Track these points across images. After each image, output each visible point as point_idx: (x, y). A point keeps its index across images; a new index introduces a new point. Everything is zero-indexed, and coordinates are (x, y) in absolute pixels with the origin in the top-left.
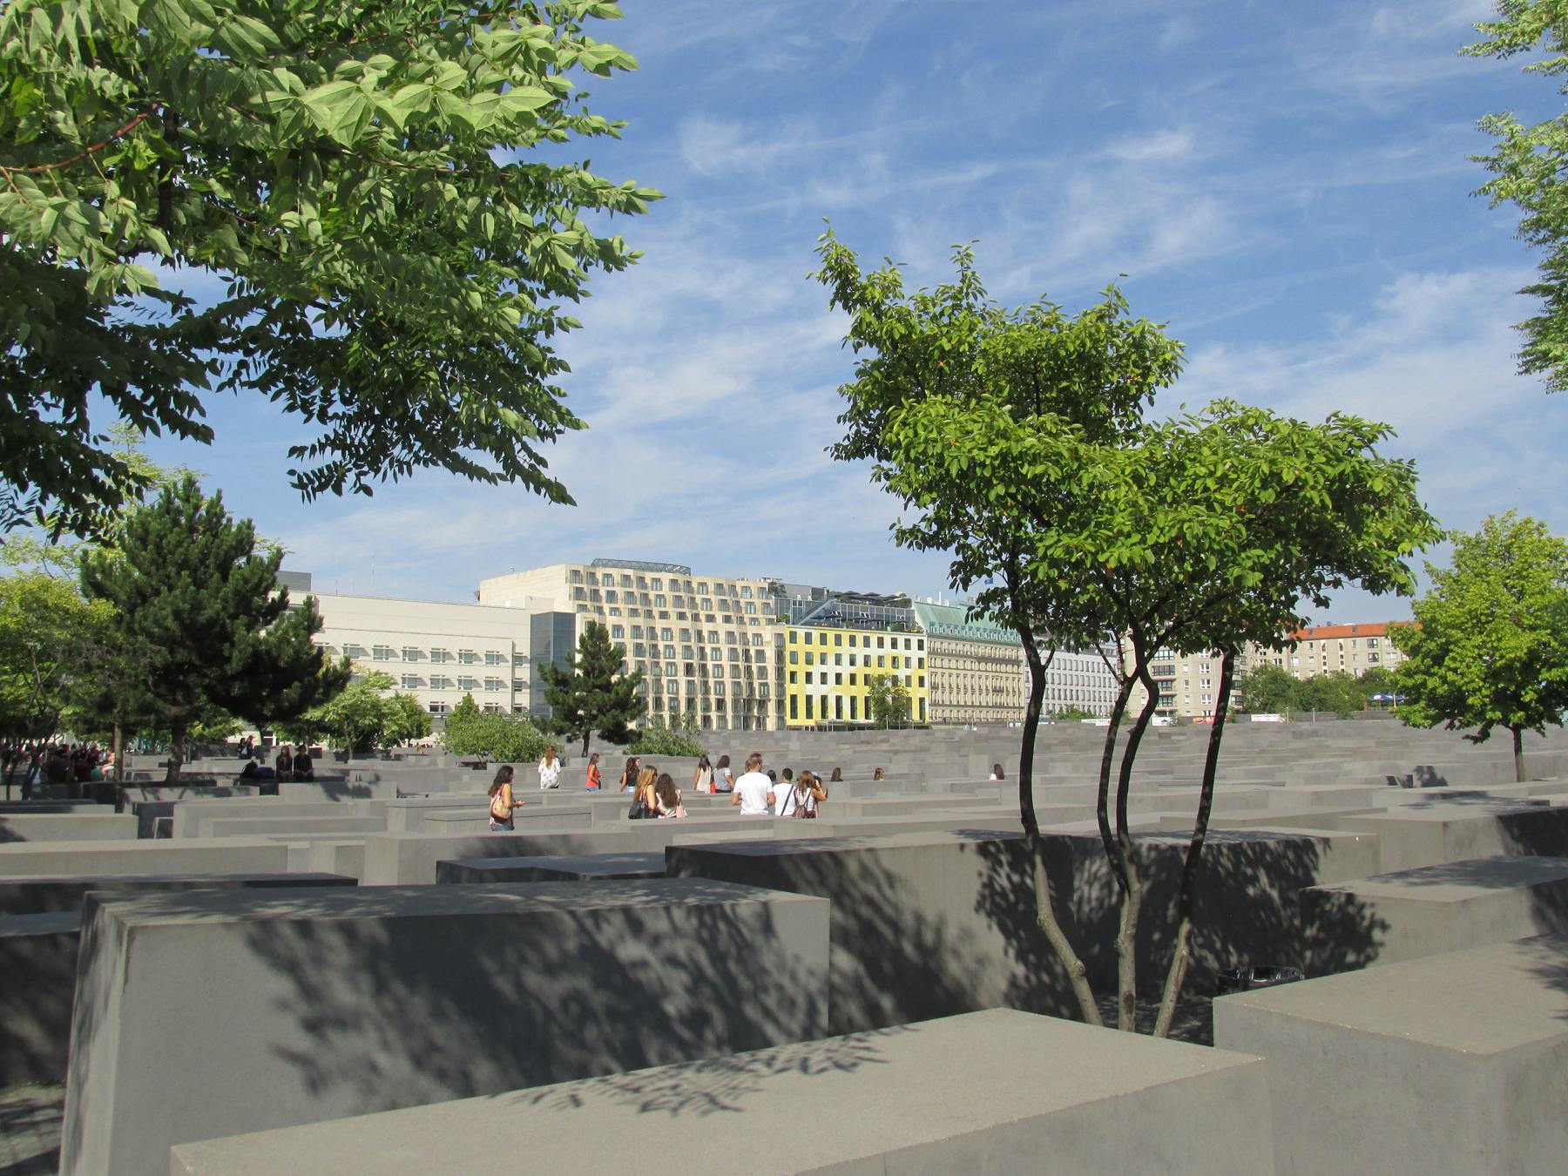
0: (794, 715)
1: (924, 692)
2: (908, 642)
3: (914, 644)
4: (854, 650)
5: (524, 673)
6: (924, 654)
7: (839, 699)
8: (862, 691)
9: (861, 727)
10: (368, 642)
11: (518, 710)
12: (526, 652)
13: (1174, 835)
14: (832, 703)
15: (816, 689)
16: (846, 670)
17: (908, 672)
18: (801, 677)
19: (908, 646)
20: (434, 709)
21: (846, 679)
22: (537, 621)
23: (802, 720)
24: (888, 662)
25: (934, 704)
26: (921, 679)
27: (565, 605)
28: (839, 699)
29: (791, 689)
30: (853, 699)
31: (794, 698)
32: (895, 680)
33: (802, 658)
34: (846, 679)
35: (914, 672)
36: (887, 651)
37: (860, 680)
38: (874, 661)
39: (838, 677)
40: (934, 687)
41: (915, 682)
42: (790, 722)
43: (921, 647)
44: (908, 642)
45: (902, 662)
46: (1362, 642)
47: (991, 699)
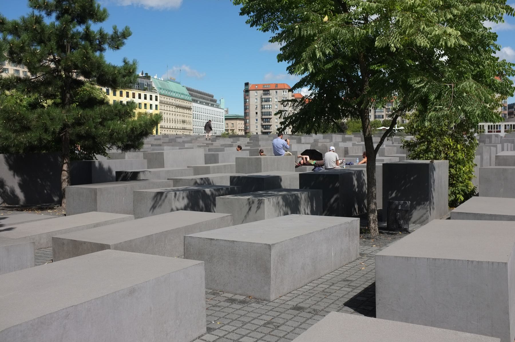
6: (157, 103)
43: (156, 100)
45: (148, 106)
47: (180, 125)
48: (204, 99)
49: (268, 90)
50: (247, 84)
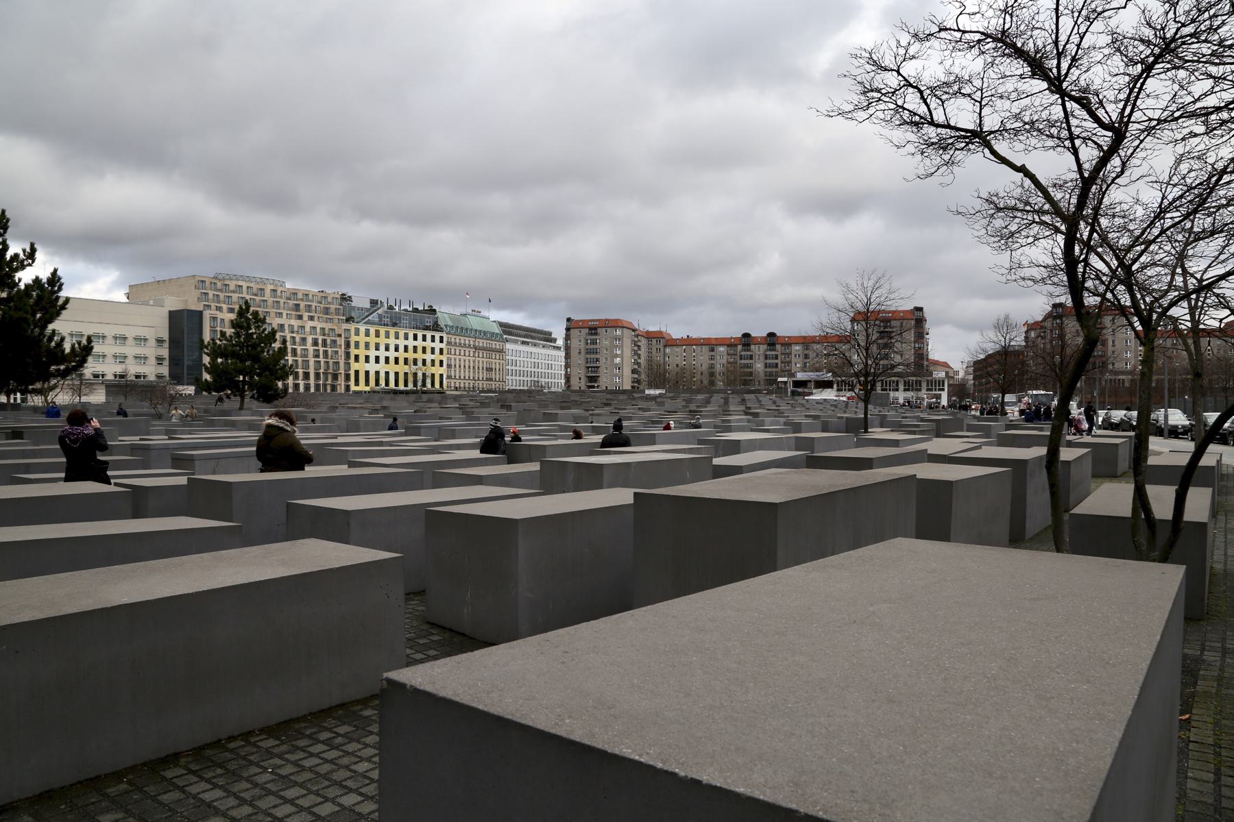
0: (357, 383)
1: (443, 370)
2: (433, 337)
3: (437, 339)
4: (397, 342)
5: (165, 352)
6: (443, 345)
7: (387, 373)
8: (402, 368)
9: (401, 392)
10: (110, 331)
11: (159, 377)
12: (166, 336)
13: (737, 470)
14: (382, 375)
15: (372, 367)
16: (392, 354)
17: (433, 357)
18: (362, 359)
19: (433, 341)
20: (96, 376)
21: (392, 360)
22: (174, 317)
23: (362, 387)
24: (420, 350)
25: (449, 377)
26: (441, 363)
27: (195, 306)
28: (387, 373)
29: (355, 366)
30: (397, 374)
31: (357, 372)
32: (424, 362)
33: (362, 345)
34: (392, 360)
35: (437, 357)
36: (420, 343)
37: (401, 361)
38: (411, 349)
39: (387, 359)
40: (449, 366)
41: (437, 363)
42: (353, 388)
43: (441, 341)
44: (433, 337)
45: (429, 351)
46: (706, 349)
48: (532, 338)
49: (595, 329)
50: (569, 320)
